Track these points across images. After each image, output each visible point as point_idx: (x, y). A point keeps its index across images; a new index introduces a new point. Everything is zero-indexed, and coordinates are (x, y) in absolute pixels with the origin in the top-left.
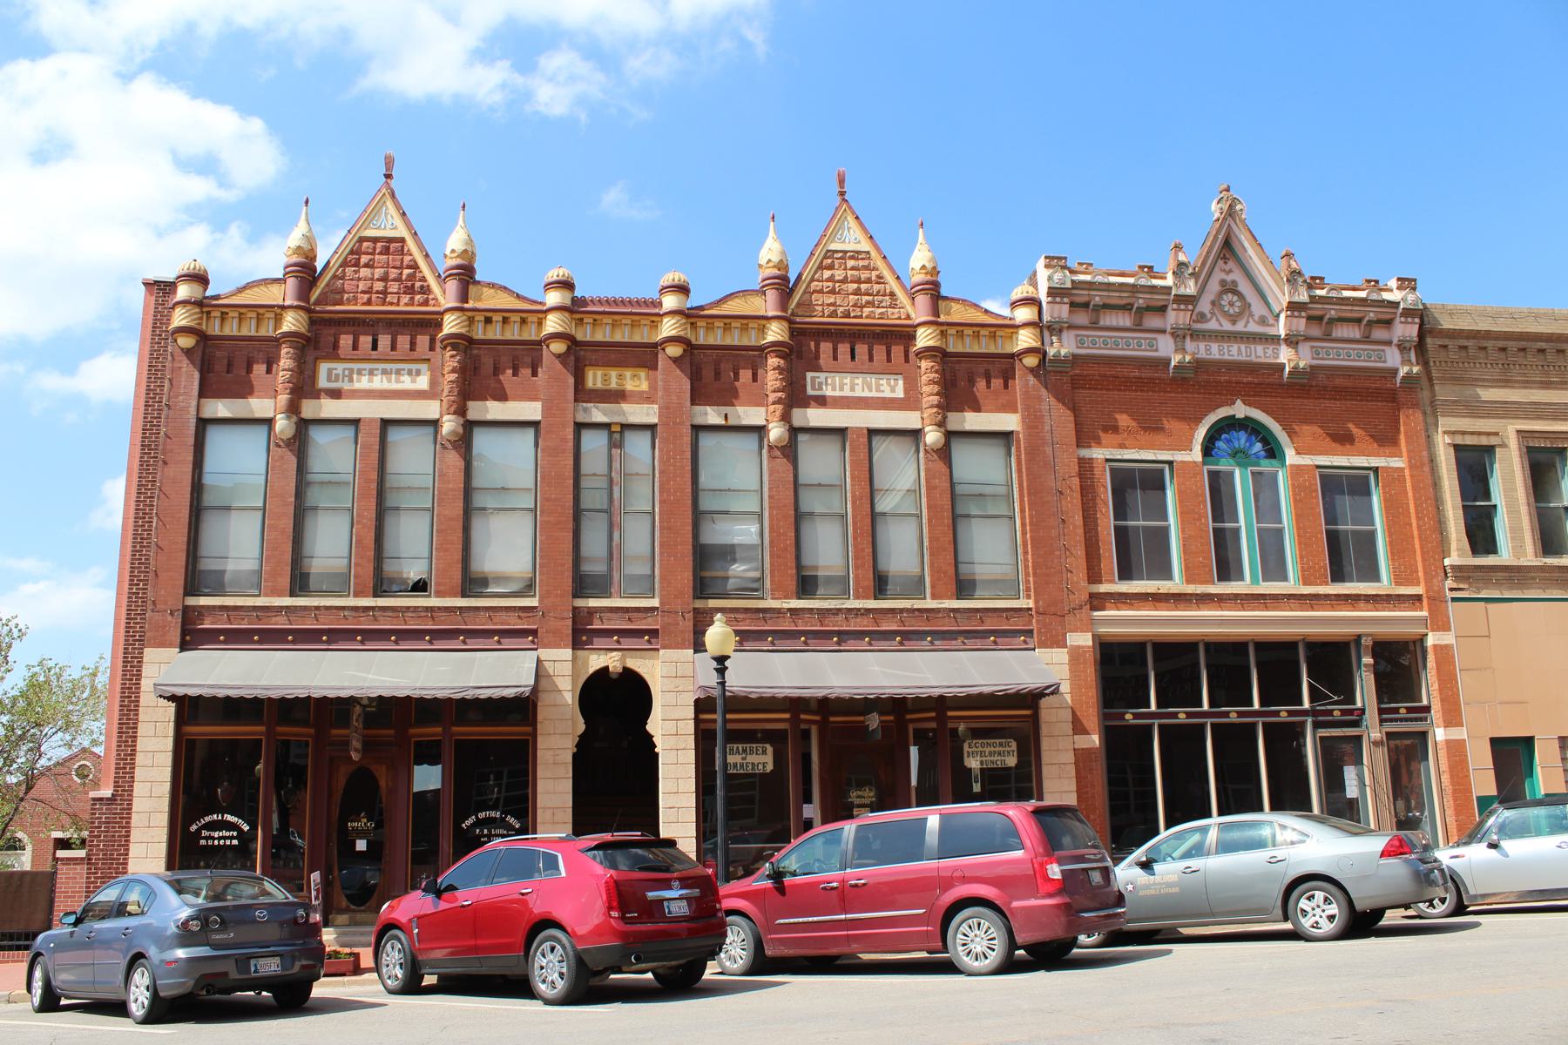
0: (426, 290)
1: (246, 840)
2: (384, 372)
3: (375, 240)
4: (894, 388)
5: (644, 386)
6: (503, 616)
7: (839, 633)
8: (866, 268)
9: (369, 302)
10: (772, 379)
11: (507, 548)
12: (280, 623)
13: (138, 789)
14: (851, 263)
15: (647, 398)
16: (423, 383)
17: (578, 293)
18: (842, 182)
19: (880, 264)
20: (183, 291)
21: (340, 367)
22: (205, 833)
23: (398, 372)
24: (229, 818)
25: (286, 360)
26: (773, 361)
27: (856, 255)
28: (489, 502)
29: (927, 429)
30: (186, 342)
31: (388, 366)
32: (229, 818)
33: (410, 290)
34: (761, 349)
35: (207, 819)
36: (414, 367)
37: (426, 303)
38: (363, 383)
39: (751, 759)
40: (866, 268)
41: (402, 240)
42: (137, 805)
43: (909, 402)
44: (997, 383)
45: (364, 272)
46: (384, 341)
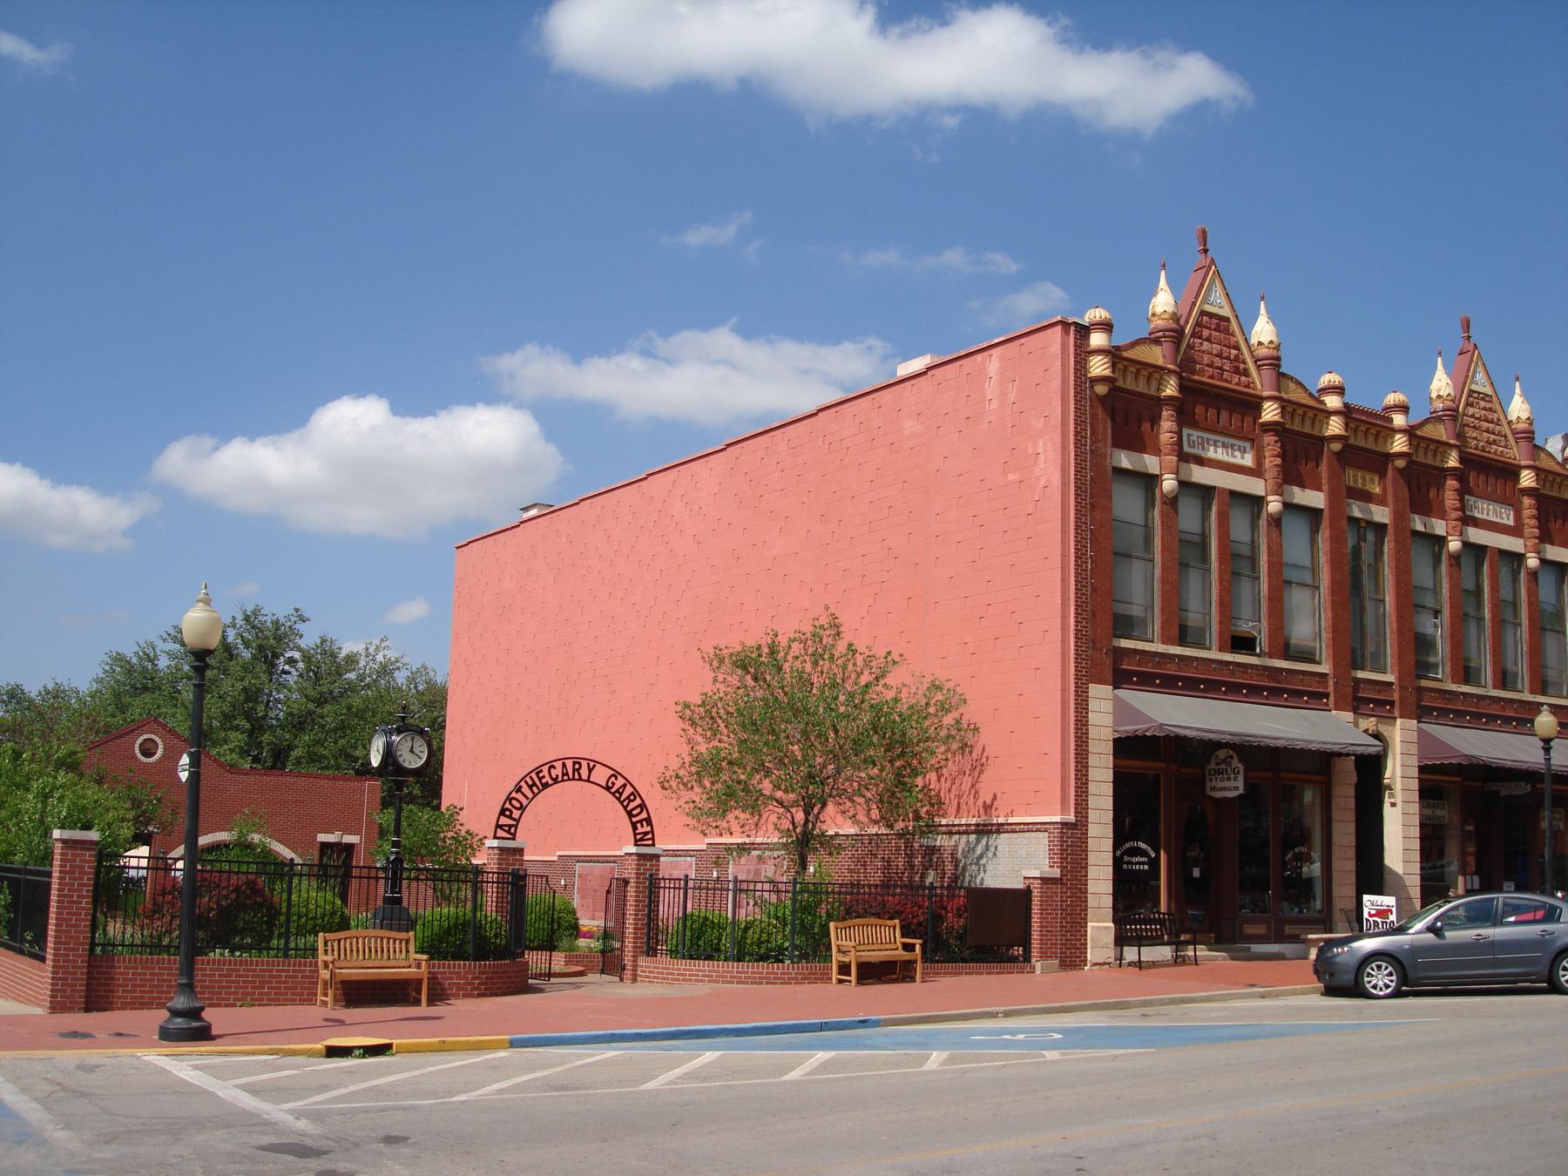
0: (1246, 373)
1: (1154, 864)
2: (1224, 446)
3: (1211, 315)
4: (1507, 517)
5: (1377, 490)
6: (1308, 679)
7: (1485, 715)
8: (1490, 410)
9: (1211, 377)
10: (1450, 498)
11: (1309, 621)
12: (1171, 670)
13: (1093, 816)
14: (1482, 404)
15: (1382, 502)
16: (1248, 460)
17: (1349, 399)
18: (1466, 325)
19: (1498, 407)
20: (1097, 339)
21: (1195, 434)
22: (1126, 858)
23: (1232, 446)
24: (1143, 845)
25: (1167, 424)
26: (1452, 483)
27: (1485, 397)
28: (1289, 574)
29: (1270, 498)
30: (1101, 389)
31: (1226, 440)
32: (1143, 845)
33: (1237, 371)
34: (1443, 470)
35: (1127, 845)
36: (1242, 444)
37: (1248, 386)
38: (1211, 453)
39: (1439, 812)
40: (1490, 410)
41: (1227, 320)
42: (1093, 830)
43: (1515, 531)
44: (1559, 522)
45: (1206, 346)
46: (1224, 414)
